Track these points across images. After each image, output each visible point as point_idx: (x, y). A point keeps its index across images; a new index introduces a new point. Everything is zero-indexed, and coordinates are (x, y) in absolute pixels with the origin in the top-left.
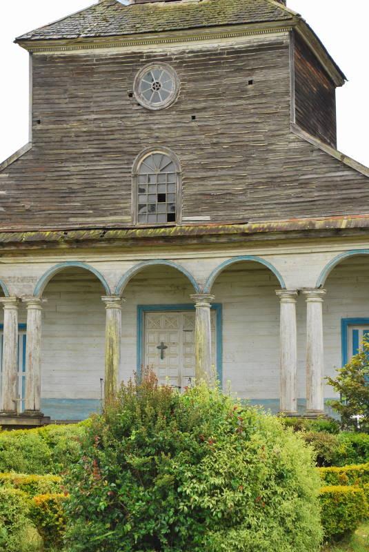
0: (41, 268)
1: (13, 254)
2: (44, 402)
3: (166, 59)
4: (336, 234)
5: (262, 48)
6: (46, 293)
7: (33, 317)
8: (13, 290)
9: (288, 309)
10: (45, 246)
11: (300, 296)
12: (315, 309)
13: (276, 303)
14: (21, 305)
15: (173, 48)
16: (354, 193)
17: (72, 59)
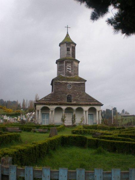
0: (55, 107)
1: (51, 105)
2: (55, 123)
3: (71, 83)
4: (90, 105)
5: (82, 83)
6: (55, 110)
7: (54, 113)
8: (51, 109)
9: (84, 113)
10: (56, 104)
11: (86, 111)
12: (87, 113)
13: (83, 112)
14: (52, 111)
15: (72, 82)
16: (91, 100)
17: (59, 82)
